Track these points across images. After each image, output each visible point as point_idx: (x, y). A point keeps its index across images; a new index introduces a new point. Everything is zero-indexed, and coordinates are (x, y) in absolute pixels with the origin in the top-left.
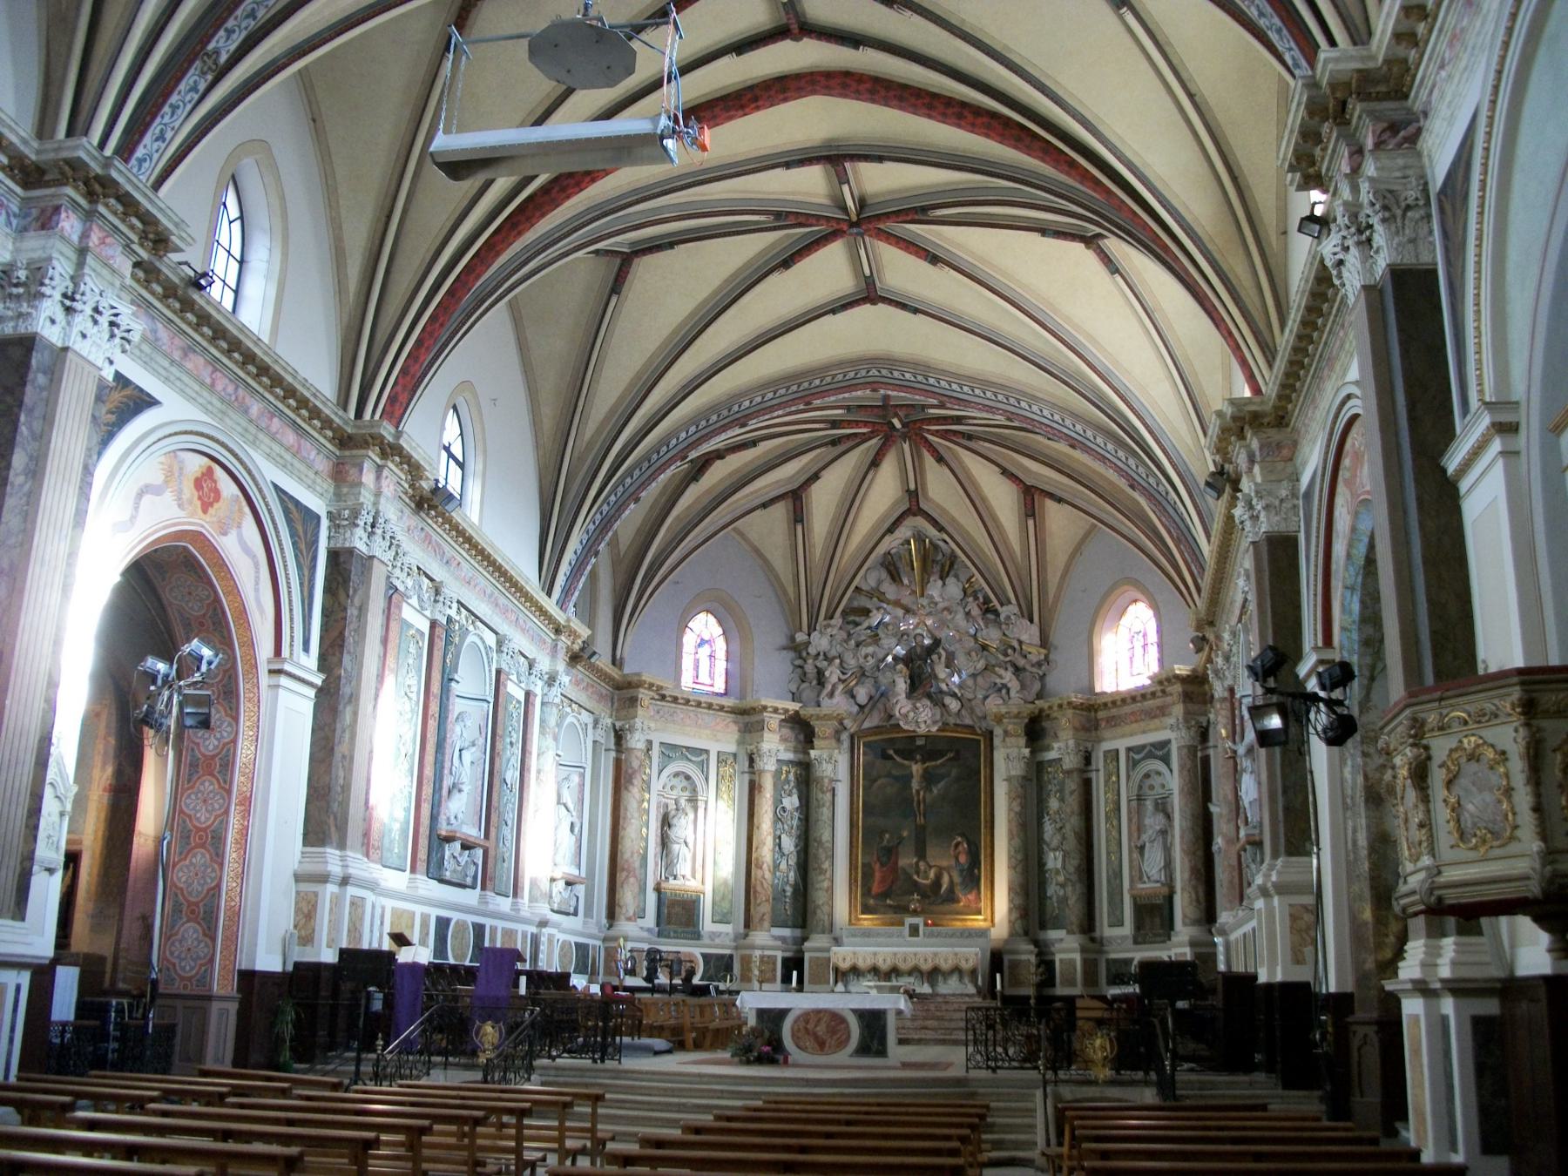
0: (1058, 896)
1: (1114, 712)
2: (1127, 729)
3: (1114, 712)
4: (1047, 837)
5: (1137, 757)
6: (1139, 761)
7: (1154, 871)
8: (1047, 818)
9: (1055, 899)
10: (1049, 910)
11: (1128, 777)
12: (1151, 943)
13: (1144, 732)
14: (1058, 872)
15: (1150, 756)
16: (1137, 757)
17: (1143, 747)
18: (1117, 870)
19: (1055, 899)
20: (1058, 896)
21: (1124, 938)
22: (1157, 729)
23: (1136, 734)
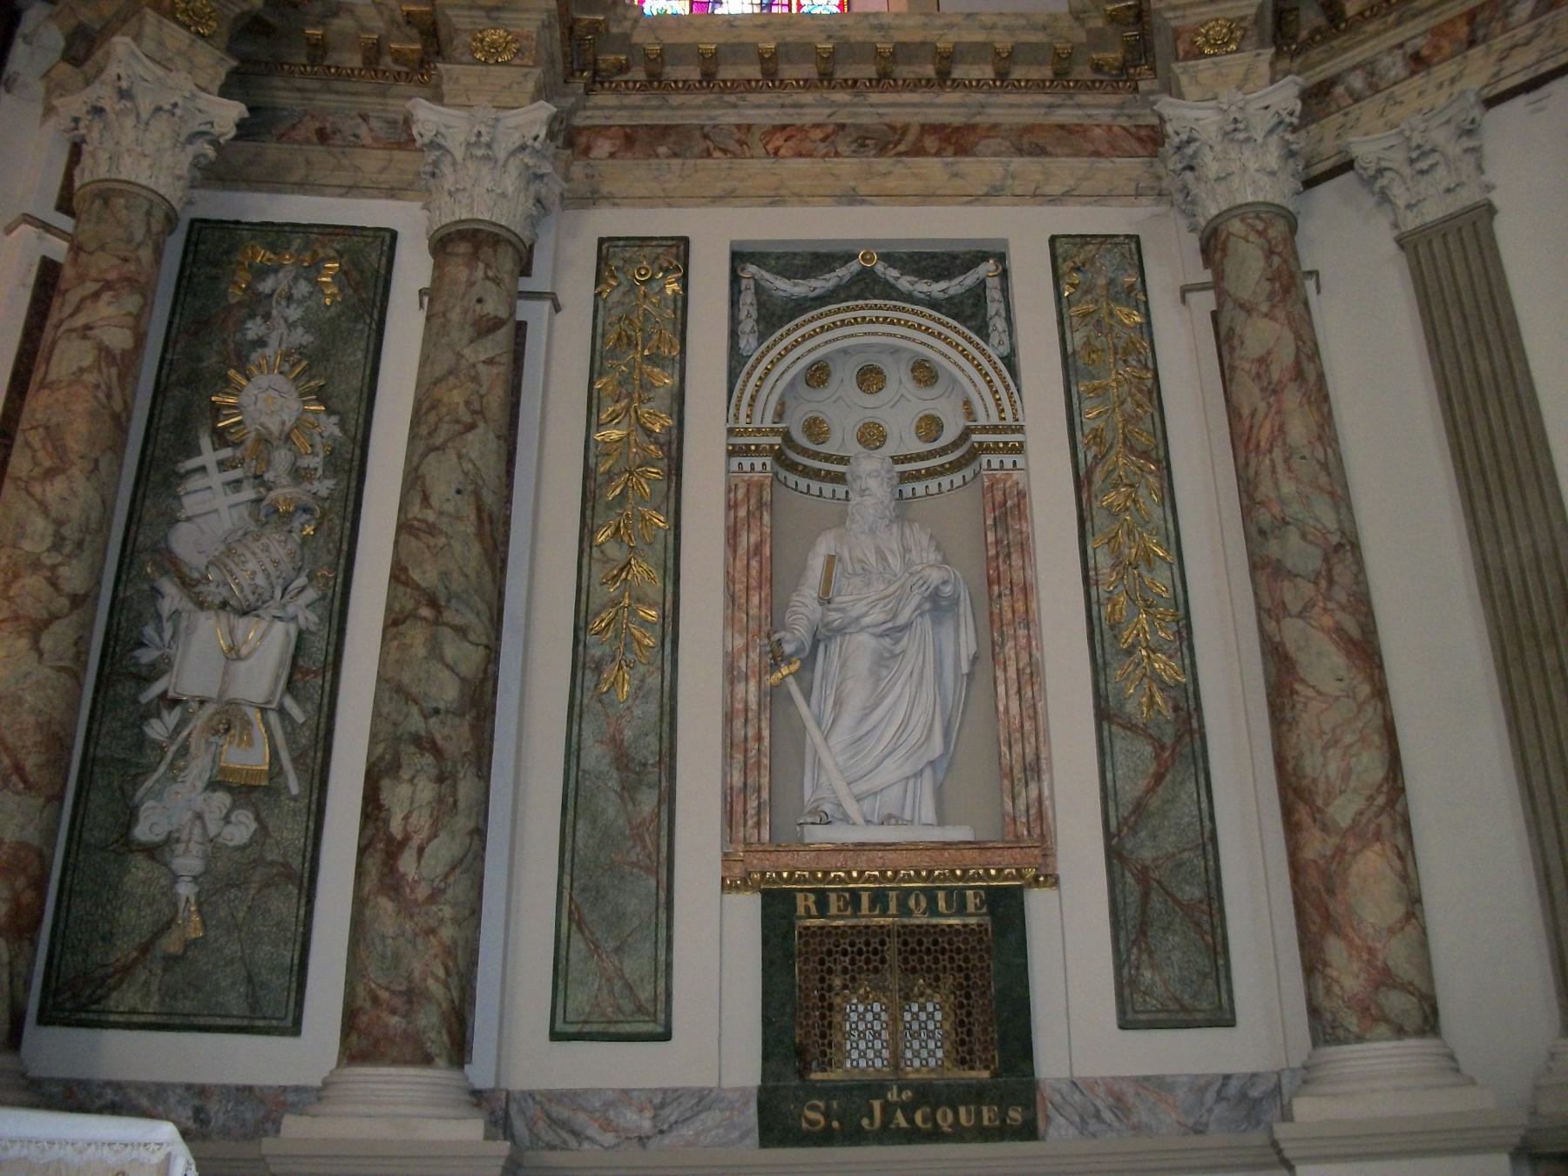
0: (214, 848)
1: (688, 110)
2: (757, 171)
3: (688, 110)
4: (186, 542)
5: (785, 287)
6: (799, 307)
7: (892, 770)
8: (208, 455)
9: (188, 862)
10: (135, 921)
11: (736, 361)
12: (912, 1136)
13: (852, 198)
14: (229, 720)
15: (866, 285)
16: (785, 287)
17: (819, 260)
18: (649, 748)
19: (188, 862)
20: (214, 848)
21: (703, 1099)
22: (927, 197)
23: (801, 198)
